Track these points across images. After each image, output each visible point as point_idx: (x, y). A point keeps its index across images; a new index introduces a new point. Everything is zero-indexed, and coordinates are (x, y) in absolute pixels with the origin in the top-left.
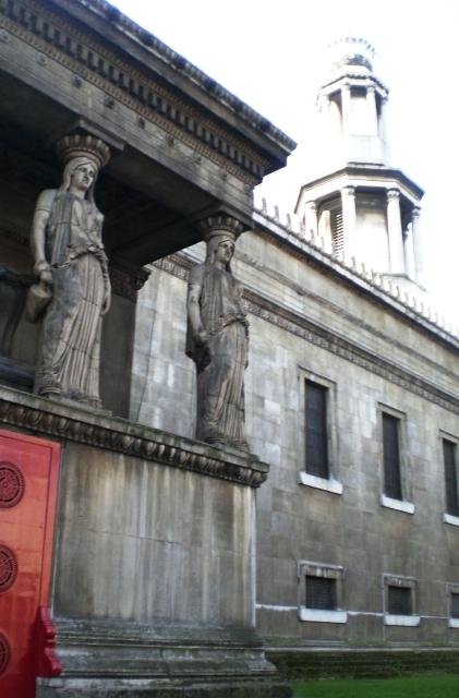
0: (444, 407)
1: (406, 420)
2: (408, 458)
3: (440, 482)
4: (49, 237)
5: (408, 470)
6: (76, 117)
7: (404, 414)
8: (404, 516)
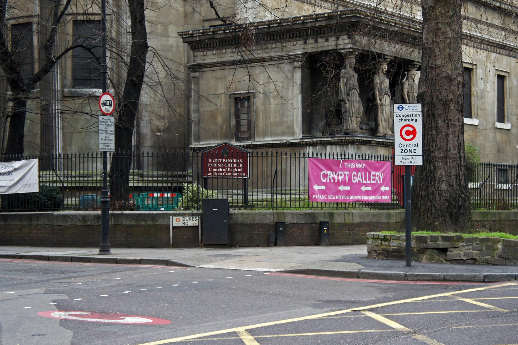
0: (500, 54)
1: (477, 69)
2: (477, 91)
3: (494, 103)
4: (409, 96)
5: (476, 99)
6: (414, 61)
7: (476, 65)
8: (473, 127)
